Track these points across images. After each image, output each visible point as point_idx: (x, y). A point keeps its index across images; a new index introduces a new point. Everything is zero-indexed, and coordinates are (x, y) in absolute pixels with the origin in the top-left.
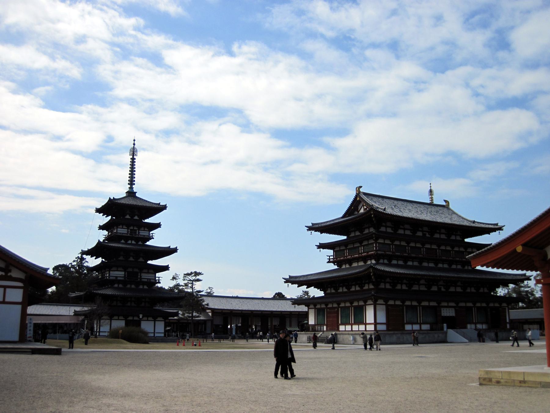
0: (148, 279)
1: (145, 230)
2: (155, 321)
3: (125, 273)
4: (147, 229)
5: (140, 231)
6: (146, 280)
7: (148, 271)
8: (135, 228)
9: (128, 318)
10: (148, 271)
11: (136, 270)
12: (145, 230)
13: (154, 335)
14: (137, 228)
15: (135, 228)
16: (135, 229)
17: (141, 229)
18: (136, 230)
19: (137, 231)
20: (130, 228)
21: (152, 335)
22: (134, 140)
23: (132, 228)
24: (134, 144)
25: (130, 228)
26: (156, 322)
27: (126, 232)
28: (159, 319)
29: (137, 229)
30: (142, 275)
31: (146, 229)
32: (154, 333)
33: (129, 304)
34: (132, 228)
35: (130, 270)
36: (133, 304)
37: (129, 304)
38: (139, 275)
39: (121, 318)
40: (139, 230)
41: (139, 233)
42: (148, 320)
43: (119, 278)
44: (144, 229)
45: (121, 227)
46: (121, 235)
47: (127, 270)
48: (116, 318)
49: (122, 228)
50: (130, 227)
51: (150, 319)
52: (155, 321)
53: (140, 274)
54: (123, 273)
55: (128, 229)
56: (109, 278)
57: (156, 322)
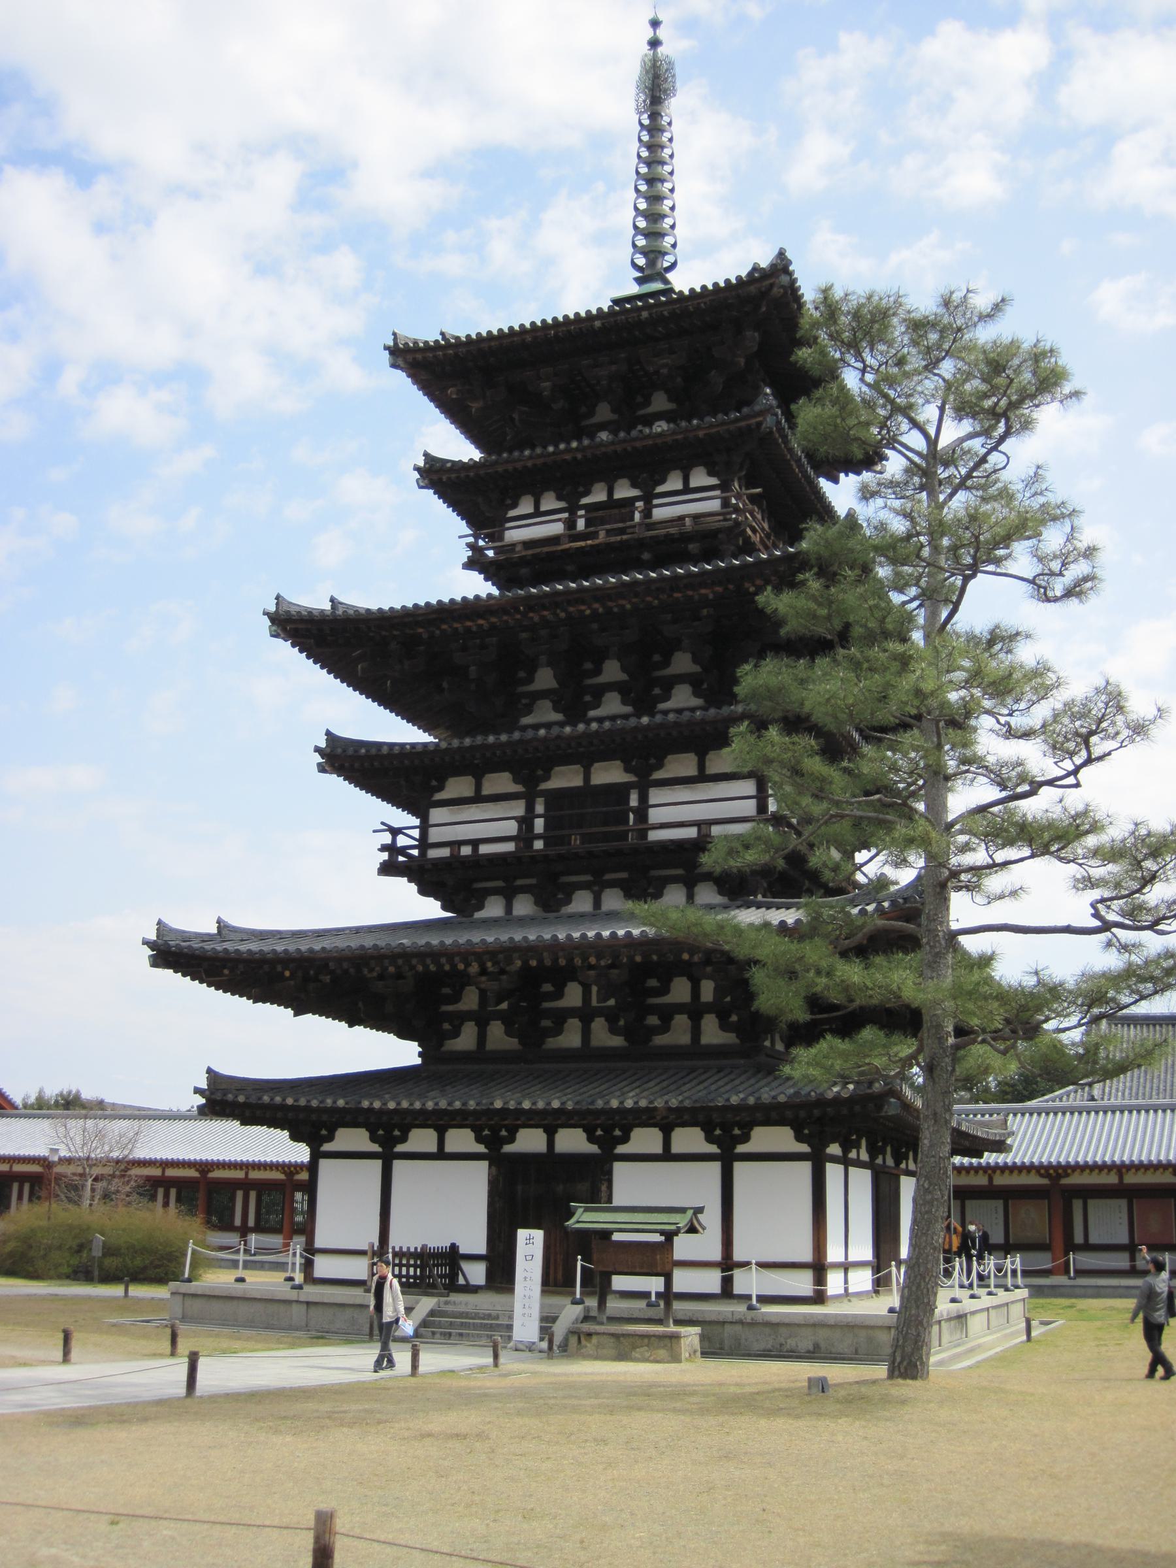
0: (698, 824)
1: (693, 484)
2: (727, 1160)
3: (530, 808)
4: (710, 474)
5: (656, 502)
6: (691, 833)
7: (701, 766)
8: (624, 491)
9: (511, 1139)
10: (701, 766)
11: (609, 774)
12: (693, 484)
13: (727, 1282)
14: (634, 485)
15: (624, 491)
16: (618, 495)
17: (660, 489)
18: (629, 502)
19: (640, 504)
20: (585, 501)
21: (710, 1281)
22: (655, 24)
23: (598, 495)
24: (654, 43)
25: (585, 501)
26: (740, 1169)
27: (557, 528)
28: (765, 1138)
29: (635, 493)
30: (652, 801)
31: (699, 478)
32: (727, 1264)
33: (571, 1038)
34: (598, 495)
35: (566, 778)
36: (603, 1036)
37: (571, 1038)
38: (634, 801)
39: (461, 1139)
40: (648, 498)
41: (647, 513)
42: (667, 1156)
43: (484, 849)
44: (686, 480)
45: (525, 507)
46: (520, 552)
47: (544, 786)
48: (422, 1139)
49: (537, 513)
50: (587, 493)
51: (689, 1139)
52: (727, 1160)
53: (644, 798)
54: (518, 808)
55: (572, 509)
56: (423, 853)
57: (739, 1168)
